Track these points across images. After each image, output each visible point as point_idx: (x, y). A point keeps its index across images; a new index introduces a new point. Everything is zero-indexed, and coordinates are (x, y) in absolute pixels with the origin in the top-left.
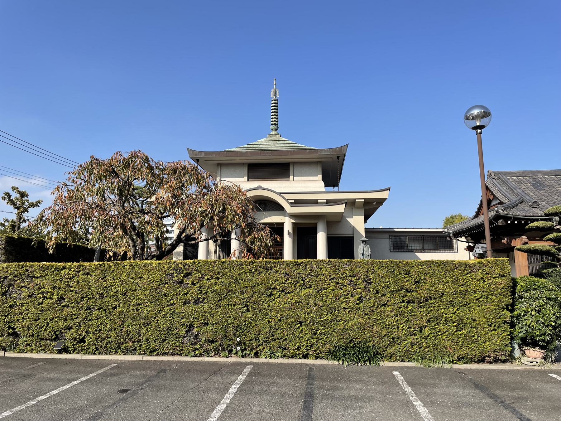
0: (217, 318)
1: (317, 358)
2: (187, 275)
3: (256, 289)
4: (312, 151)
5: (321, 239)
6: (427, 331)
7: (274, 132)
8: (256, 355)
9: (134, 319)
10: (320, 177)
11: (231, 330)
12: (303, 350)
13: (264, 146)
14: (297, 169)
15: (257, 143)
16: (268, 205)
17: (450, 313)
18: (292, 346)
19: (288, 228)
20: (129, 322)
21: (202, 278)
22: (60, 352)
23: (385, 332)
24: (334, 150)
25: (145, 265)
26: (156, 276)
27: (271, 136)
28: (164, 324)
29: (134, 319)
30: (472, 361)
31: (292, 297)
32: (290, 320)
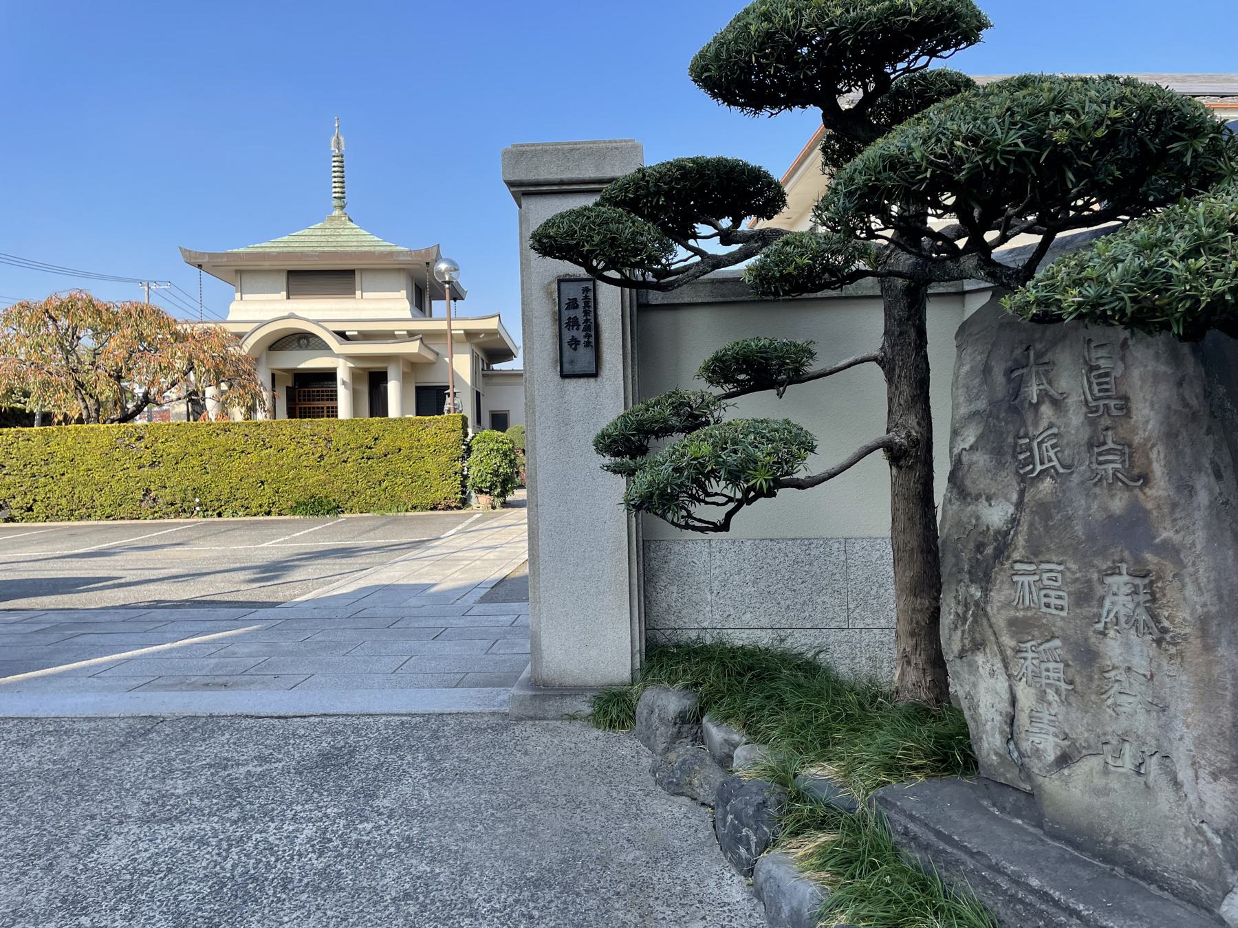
0: (173, 481)
1: (280, 514)
2: (140, 438)
3: (215, 451)
4: (383, 255)
5: (393, 389)
6: (384, 485)
7: (337, 213)
8: (220, 515)
9: (85, 485)
10: (403, 293)
11: (190, 493)
12: (266, 508)
13: (316, 239)
14: (368, 279)
15: (306, 232)
16: (302, 340)
17: (405, 466)
18: (254, 504)
19: (342, 375)
20: (80, 488)
21: (156, 440)
22: (7, 521)
23: (345, 486)
24: (418, 253)
25: (92, 429)
26: (105, 440)
27: (332, 219)
28: (119, 489)
29: (85, 485)
30: (424, 508)
31: (253, 458)
32: (251, 480)
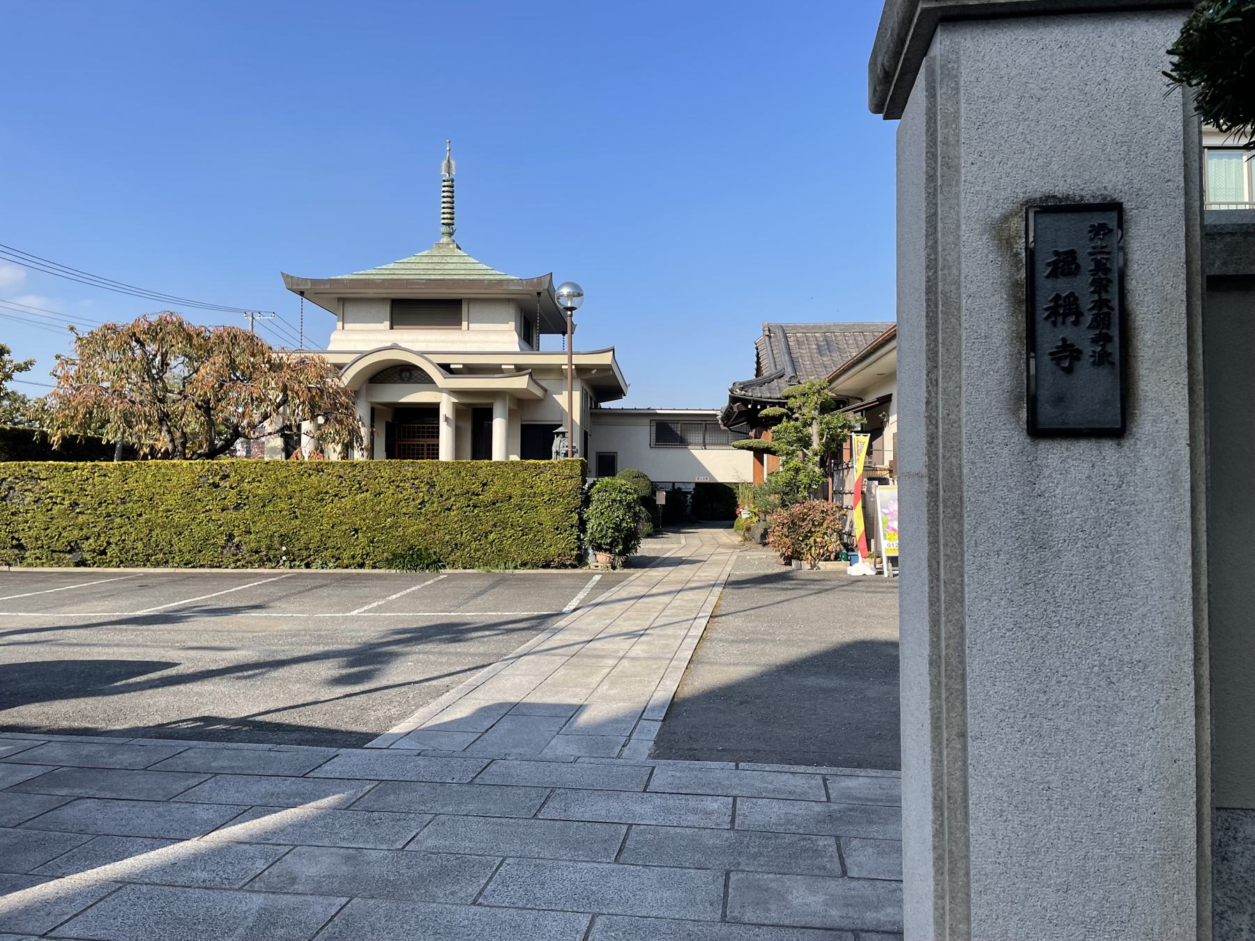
1: (374, 567)
2: (225, 477)
3: (306, 493)
5: (499, 427)
6: (491, 537)
7: (445, 240)
8: (308, 566)
9: (163, 527)
10: (512, 325)
11: (276, 540)
12: (358, 559)
14: (475, 310)
15: (413, 259)
16: (405, 372)
17: (515, 517)
18: (346, 555)
19: (446, 410)
20: (158, 531)
22: (77, 565)
23: (448, 537)
24: (530, 282)
25: (174, 466)
26: (187, 478)
27: (440, 246)
28: (198, 533)
29: (163, 527)
30: (535, 566)
31: (347, 503)
32: (344, 528)
